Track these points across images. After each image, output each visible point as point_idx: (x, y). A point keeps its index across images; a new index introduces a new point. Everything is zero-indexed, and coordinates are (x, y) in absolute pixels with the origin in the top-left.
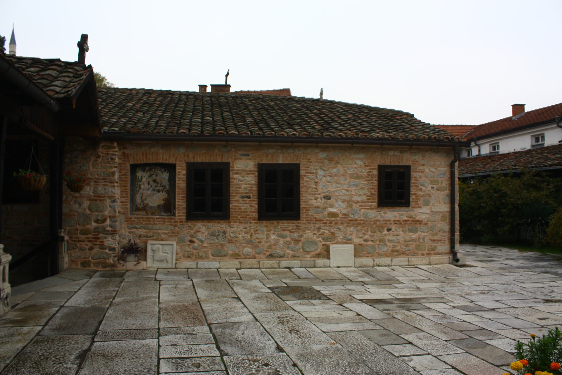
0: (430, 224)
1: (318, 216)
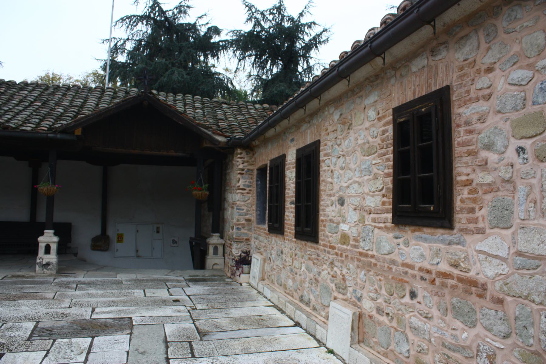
0: (512, 307)
1: (334, 239)
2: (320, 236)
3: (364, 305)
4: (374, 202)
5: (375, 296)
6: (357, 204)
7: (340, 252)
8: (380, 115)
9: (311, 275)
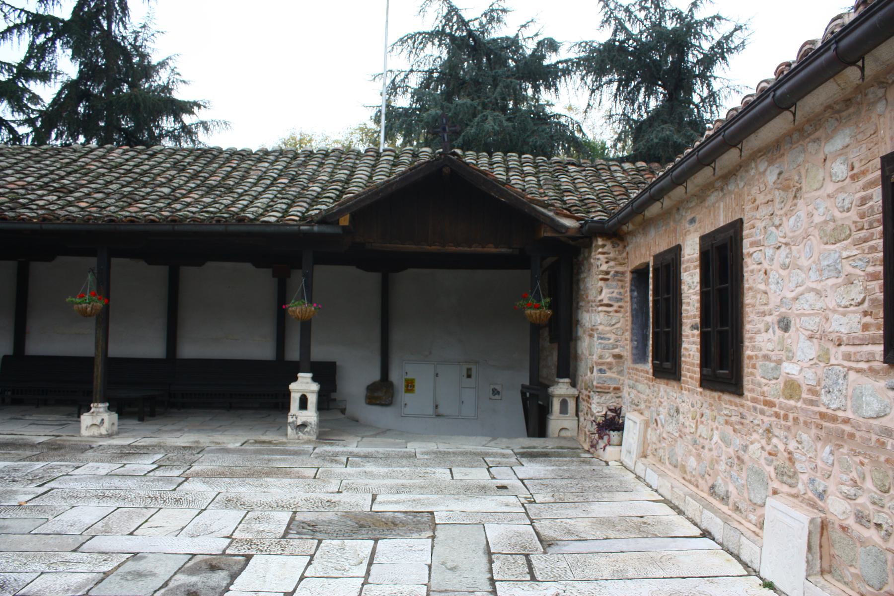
1: (772, 389)
2: (745, 383)
3: (830, 506)
4: (847, 324)
5: (852, 491)
6: (815, 328)
7: (782, 413)
8: (855, 171)
9: (731, 450)
